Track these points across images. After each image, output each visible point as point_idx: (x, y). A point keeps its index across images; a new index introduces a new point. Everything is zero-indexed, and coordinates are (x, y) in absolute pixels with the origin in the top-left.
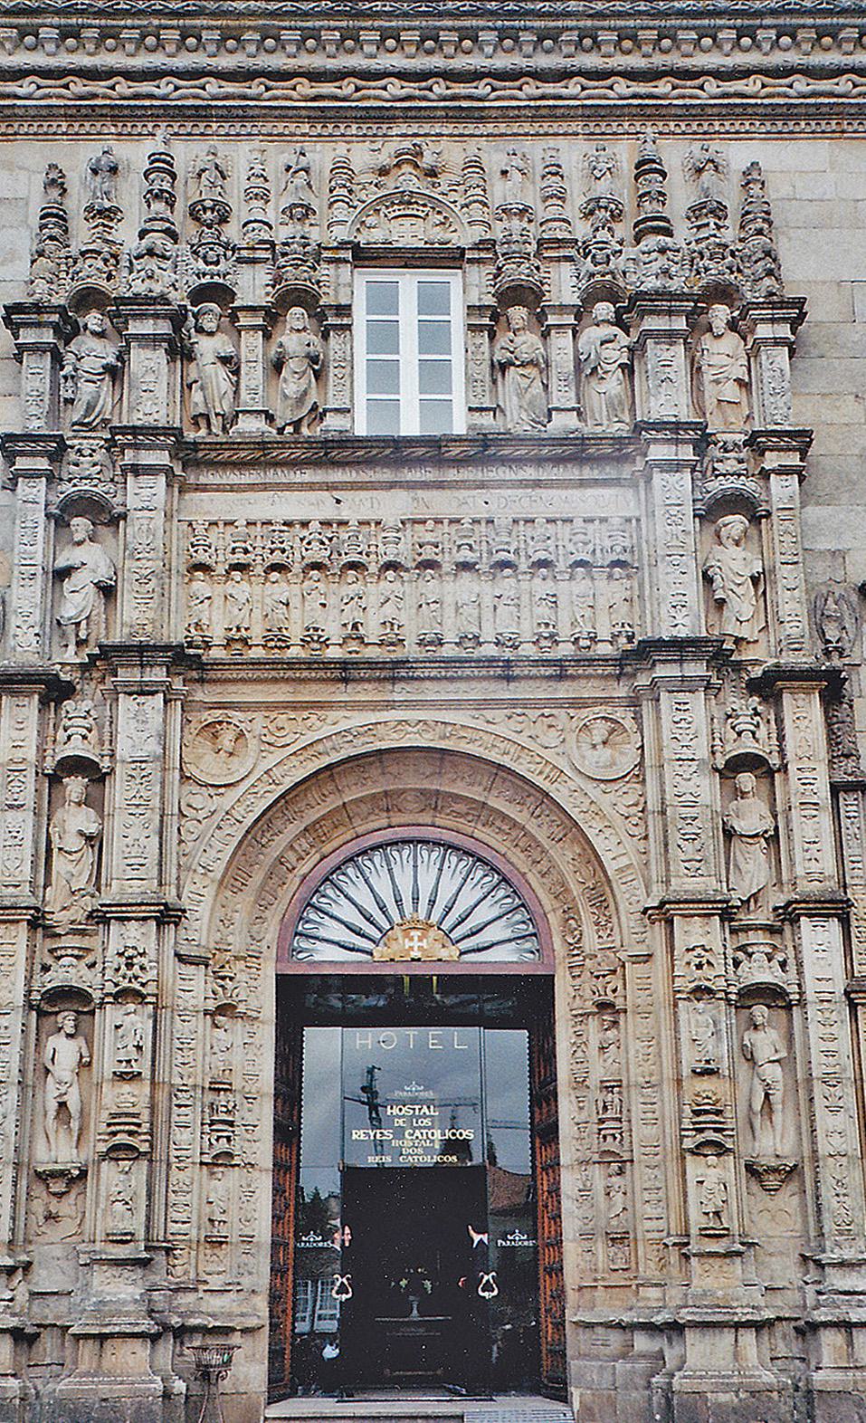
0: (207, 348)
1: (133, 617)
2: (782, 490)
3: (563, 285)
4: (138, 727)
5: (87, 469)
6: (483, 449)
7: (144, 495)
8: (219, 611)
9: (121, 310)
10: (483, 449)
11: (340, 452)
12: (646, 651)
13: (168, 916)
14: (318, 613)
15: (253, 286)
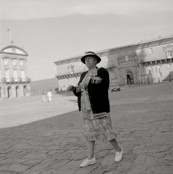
0: (122, 59)
1: (121, 67)
2: (137, 61)
3: (131, 56)
4: (121, 70)
5: (119, 63)
6: (129, 61)
7: (121, 64)
8: (123, 66)
9: (120, 59)
10: (129, 61)
11: (126, 62)
12: (133, 66)
13: (123, 74)
14: (125, 66)
15: (123, 57)
